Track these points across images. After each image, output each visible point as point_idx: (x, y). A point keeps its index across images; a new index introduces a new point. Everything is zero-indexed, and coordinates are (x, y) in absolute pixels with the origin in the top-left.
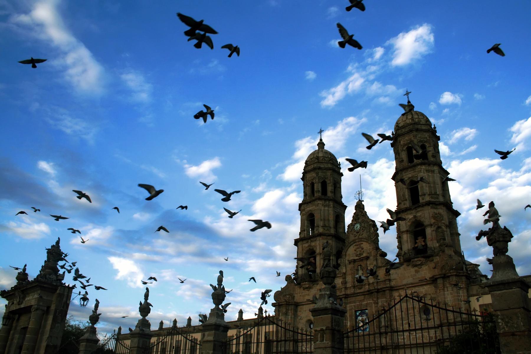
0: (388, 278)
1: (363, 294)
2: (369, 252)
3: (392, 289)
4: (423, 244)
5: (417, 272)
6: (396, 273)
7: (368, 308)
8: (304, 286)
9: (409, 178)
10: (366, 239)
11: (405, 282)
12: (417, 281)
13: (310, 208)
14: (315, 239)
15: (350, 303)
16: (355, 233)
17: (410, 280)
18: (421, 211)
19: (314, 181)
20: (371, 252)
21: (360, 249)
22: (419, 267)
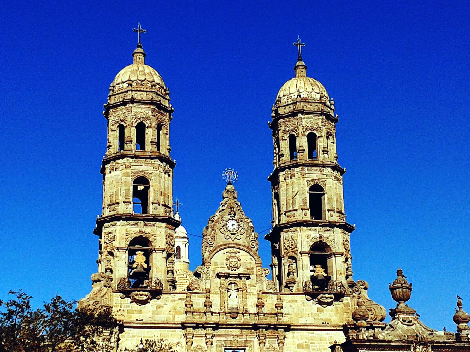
0: (279, 311)
1: (242, 327)
2: (249, 267)
3: (288, 328)
4: (325, 275)
5: (318, 310)
6: (291, 306)
7: (247, 348)
8: (137, 297)
9: (314, 180)
10: (248, 248)
11: (302, 321)
12: (320, 323)
13: (142, 168)
14: (153, 223)
15: (219, 336)
16: (228, 233)
17: (310, 321)
18: (328, 230)
19: (147, 124)
20: (252, 268)
21: (236, 260)
22: (324, 306)
